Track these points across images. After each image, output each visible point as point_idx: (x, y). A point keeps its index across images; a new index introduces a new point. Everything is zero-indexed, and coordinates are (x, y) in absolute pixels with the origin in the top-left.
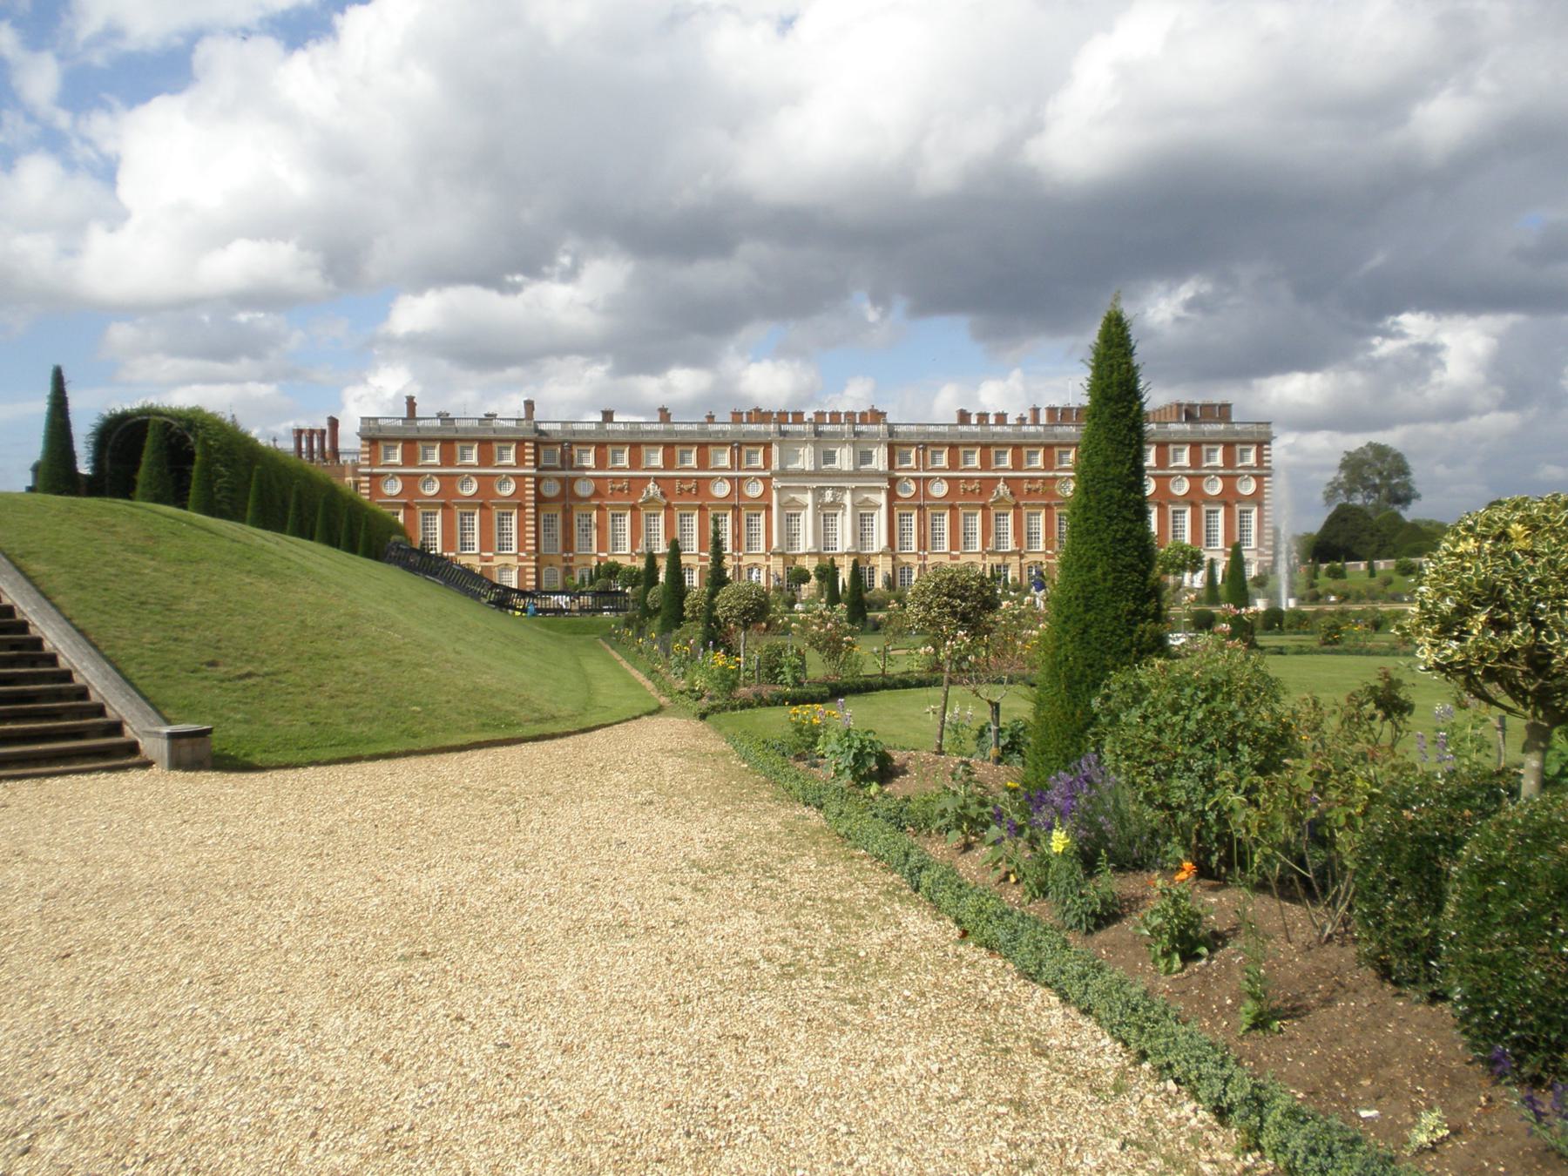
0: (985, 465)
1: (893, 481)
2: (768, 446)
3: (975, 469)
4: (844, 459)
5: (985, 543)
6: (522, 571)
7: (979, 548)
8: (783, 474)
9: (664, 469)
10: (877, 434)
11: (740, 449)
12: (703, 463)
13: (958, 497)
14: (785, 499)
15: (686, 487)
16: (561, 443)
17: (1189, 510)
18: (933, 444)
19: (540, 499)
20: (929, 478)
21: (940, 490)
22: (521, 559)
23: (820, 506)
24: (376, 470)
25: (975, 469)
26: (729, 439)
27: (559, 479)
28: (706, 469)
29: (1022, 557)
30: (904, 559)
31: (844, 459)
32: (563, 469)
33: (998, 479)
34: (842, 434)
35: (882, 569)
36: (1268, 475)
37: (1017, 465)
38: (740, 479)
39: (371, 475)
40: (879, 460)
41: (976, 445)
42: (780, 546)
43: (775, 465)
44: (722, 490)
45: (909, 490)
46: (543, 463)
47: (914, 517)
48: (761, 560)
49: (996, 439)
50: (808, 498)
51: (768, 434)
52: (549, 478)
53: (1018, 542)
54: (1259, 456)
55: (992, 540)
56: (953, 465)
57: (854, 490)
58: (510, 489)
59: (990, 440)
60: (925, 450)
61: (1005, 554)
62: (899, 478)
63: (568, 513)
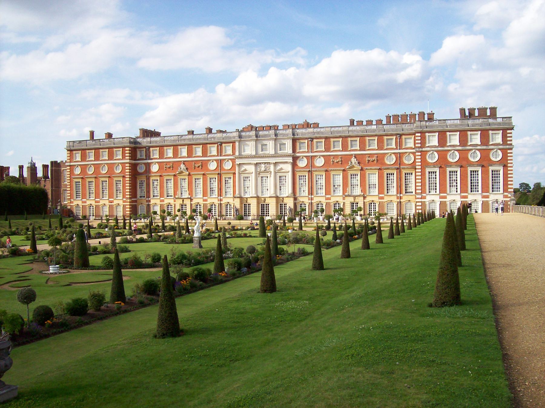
0: (345, 148)
1: (295, 159)
2: (234, 143)
3: (339, 151)
4: (270, 149)
5: (344, 191)
6: (124, 206)
7: (341, 194)
8: (241, 157)
9: (188, 157)
10: (287, 135)
11: (221, 145)
12: (205, 153)
13: (330, 166)
14: (243, 169)
15: (197, 165)
16: (145, 147)
17: (458, 170)
18: (317, 138)
19: (135, 174)
20: (316, 156)
21: (320, 162)
22: (124, 202)
23: (258, 173)
24: (71, 164)
25: (339, 151)
26: (216, 141)
27: (145, 164)
28: (206, 156)
29: (364, 198)
30: (301, 199)
31: (270, 149)
32: (146, 159)
33: (352, 155)
34: (270, 136)
35: (290, 203)
36: (511, 149)
37: (362, 148)
38: (221, 161)
39: (70, 166)
40: (288, 150)
41: (340, 137)
42: (240, 193)
43: (237, 153)
44: (213, 166)
45: (303, 163)
46: (139, 157)
47: (307, 177)
48: (231, 201)
49: (351, 134)
50: (251, 169)
51: (234, 137)
52: (141, 164)
53: (363, 190)
54: (504, 137)
55: (349, 189)
56: (327, 149)
57: (276, 164)
58: (119, 170)
59: (347, 134)
60: (312, 141)
61: (355, 197)
62: (298, 157)
63: (148, 179)
